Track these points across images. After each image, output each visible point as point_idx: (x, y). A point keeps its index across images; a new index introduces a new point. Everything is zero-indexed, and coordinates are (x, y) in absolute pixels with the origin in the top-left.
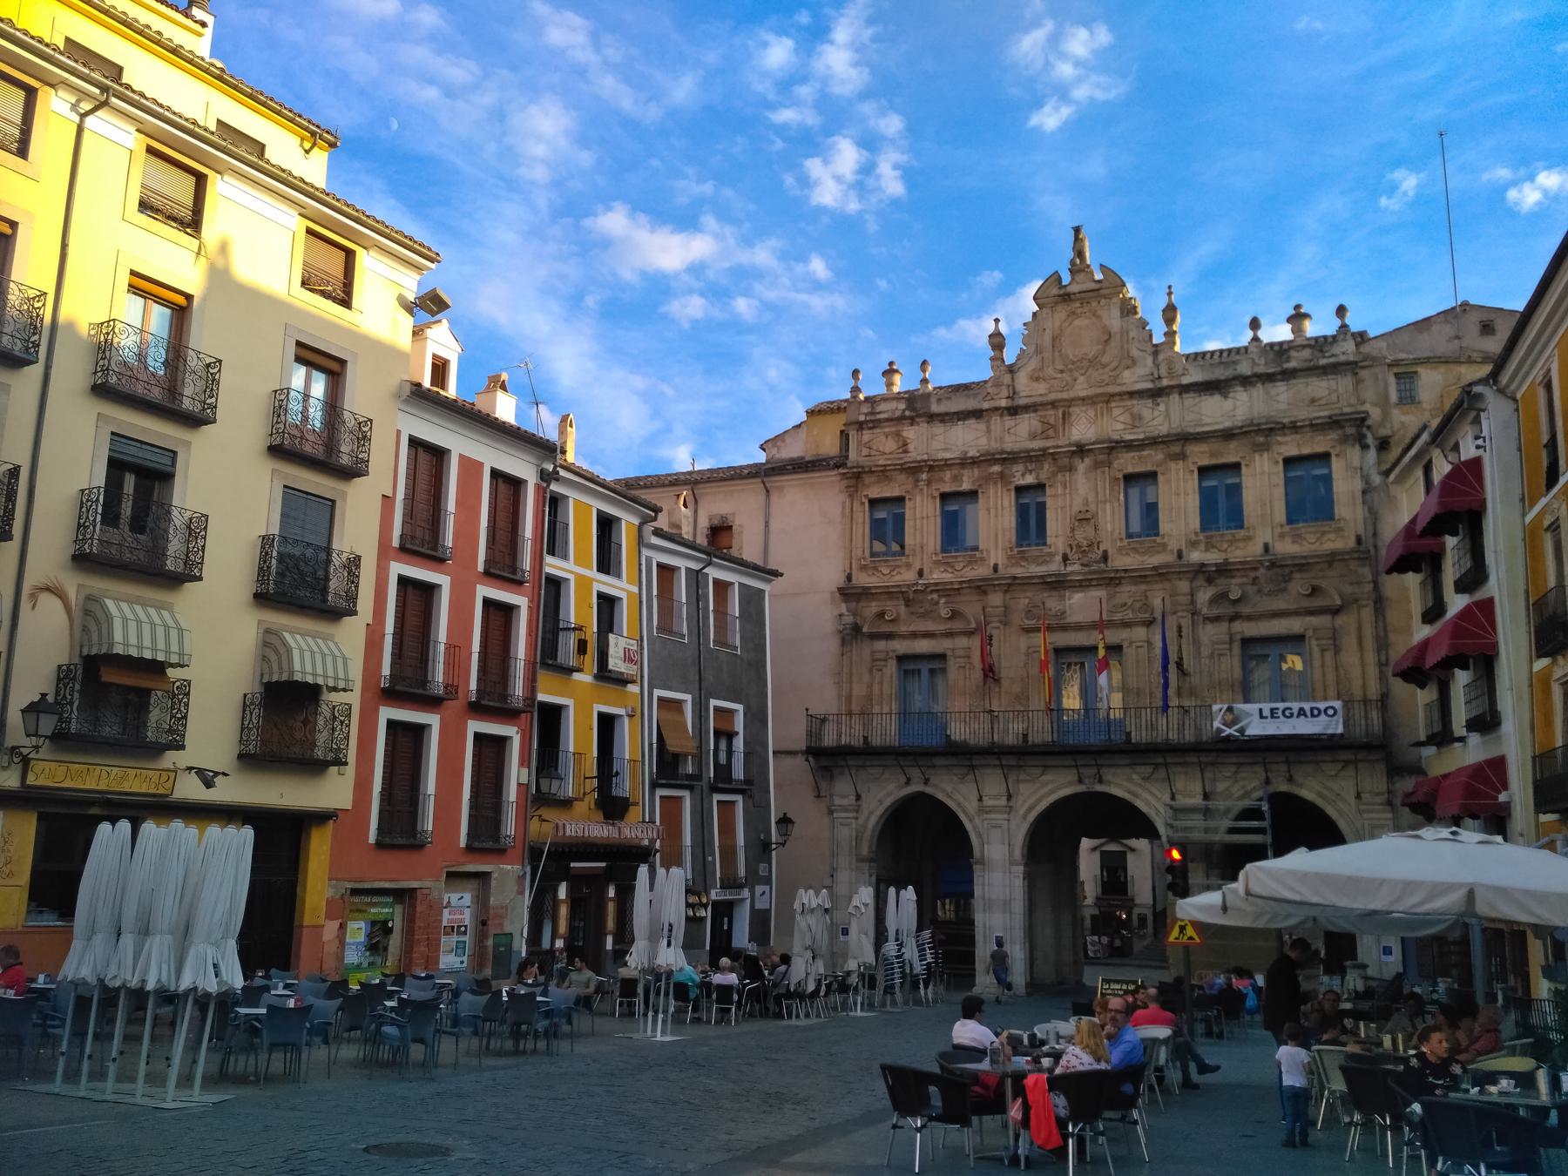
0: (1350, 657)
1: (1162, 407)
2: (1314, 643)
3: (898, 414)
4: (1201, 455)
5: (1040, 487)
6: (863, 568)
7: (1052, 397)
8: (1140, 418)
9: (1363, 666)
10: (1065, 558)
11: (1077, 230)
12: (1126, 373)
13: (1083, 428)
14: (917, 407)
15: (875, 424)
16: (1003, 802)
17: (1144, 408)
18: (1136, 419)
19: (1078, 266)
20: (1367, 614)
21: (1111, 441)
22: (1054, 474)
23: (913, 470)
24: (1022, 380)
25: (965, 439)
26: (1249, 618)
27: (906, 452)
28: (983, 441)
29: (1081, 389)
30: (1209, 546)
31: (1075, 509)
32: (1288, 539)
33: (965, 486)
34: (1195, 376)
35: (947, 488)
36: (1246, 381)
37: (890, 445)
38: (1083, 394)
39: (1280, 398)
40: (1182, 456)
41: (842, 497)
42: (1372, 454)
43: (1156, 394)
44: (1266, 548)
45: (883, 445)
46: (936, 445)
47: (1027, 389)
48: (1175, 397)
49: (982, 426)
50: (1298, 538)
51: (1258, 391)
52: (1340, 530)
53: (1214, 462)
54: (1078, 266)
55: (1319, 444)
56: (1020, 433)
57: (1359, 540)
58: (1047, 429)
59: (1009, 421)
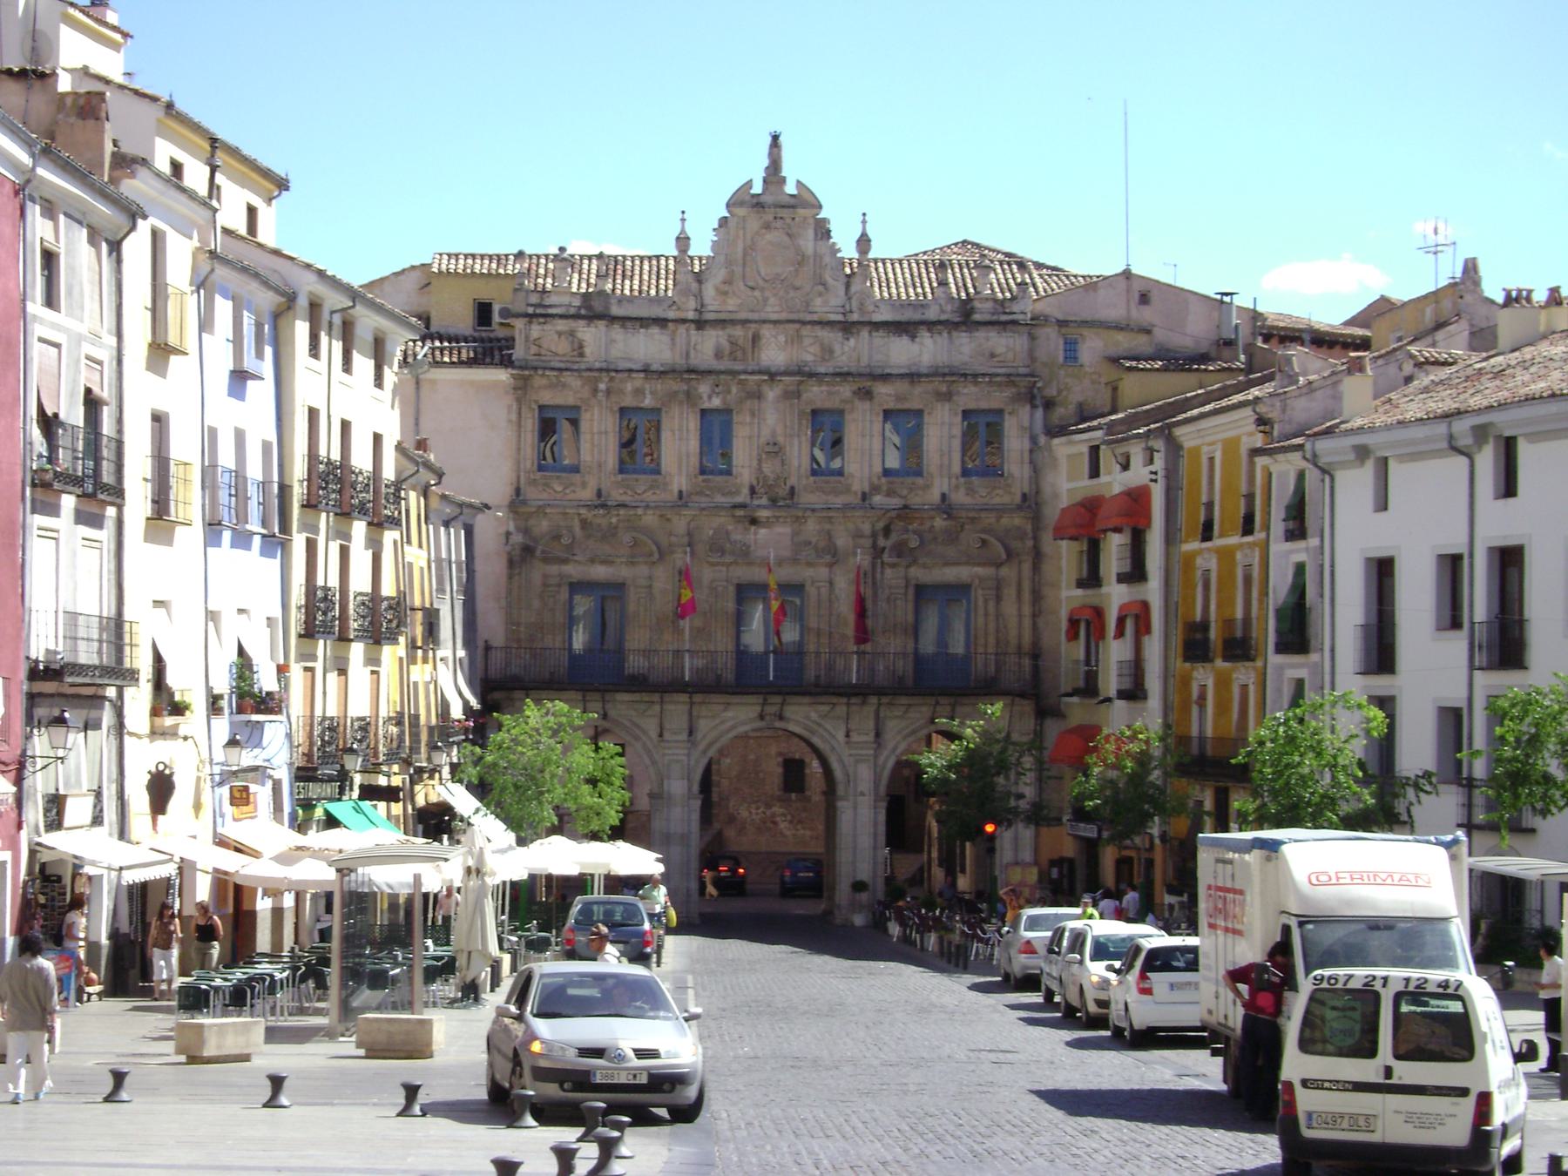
0: (1009, 608)
1: (852, 342)
2: (980, 592)
3: (572, 311)
6: (533, 482)
7: (743, 315)
8: (831, 352)
9: (1020, 616)
10: (753, 491)
11: (775, 138)
12: (818, 301)
13: (774, 353)
14: (594, 309)
16: (684, 736)
18: (827, 351)
20: (1027, 567)
21: (799, 372)
22: (741, 401)
26: (924, 566)
27: (582, 355)
29: (772, 310)
30: (889, 494)
31: (763, 440)
32: (962, 491)
33: (648, 402)
35: (628, 401)
36: (931, 325)
38: (774, 317)
41: (509, 400)
42: (1039, 413)
43: (847, 327)
44: (944, 496)
48: (865, 333)
50: (970, 491)
51: (943, 339)
52: (1009, 486)
53: (899, 406)
55: (996, 398)
56: (706, 348)
57: (1024, 496)
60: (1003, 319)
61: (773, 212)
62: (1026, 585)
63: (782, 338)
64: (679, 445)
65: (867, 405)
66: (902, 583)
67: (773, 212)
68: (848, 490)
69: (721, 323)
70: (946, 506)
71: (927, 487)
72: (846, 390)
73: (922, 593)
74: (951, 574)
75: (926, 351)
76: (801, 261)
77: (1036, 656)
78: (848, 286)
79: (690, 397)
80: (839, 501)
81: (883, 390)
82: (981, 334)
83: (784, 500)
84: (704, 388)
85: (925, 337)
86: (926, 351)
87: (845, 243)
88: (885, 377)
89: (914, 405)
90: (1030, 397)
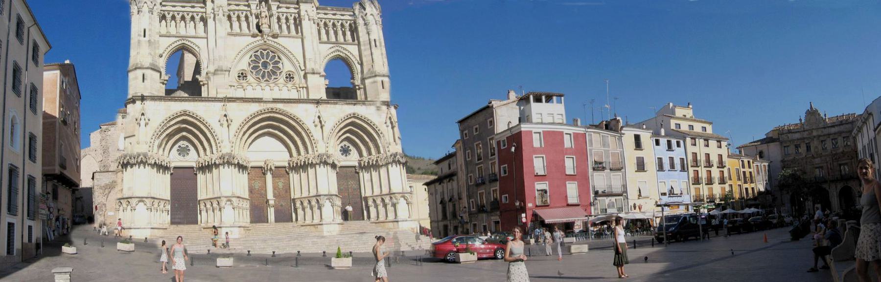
13: (815, 133)
14: (790, 132)
23: (790, 141)
47: (806, 128)
56: (805, 134)
61: (812, 113)
67: (812, 113)
73: (840, 165)
83: (820, 156)
87: (822, 115)
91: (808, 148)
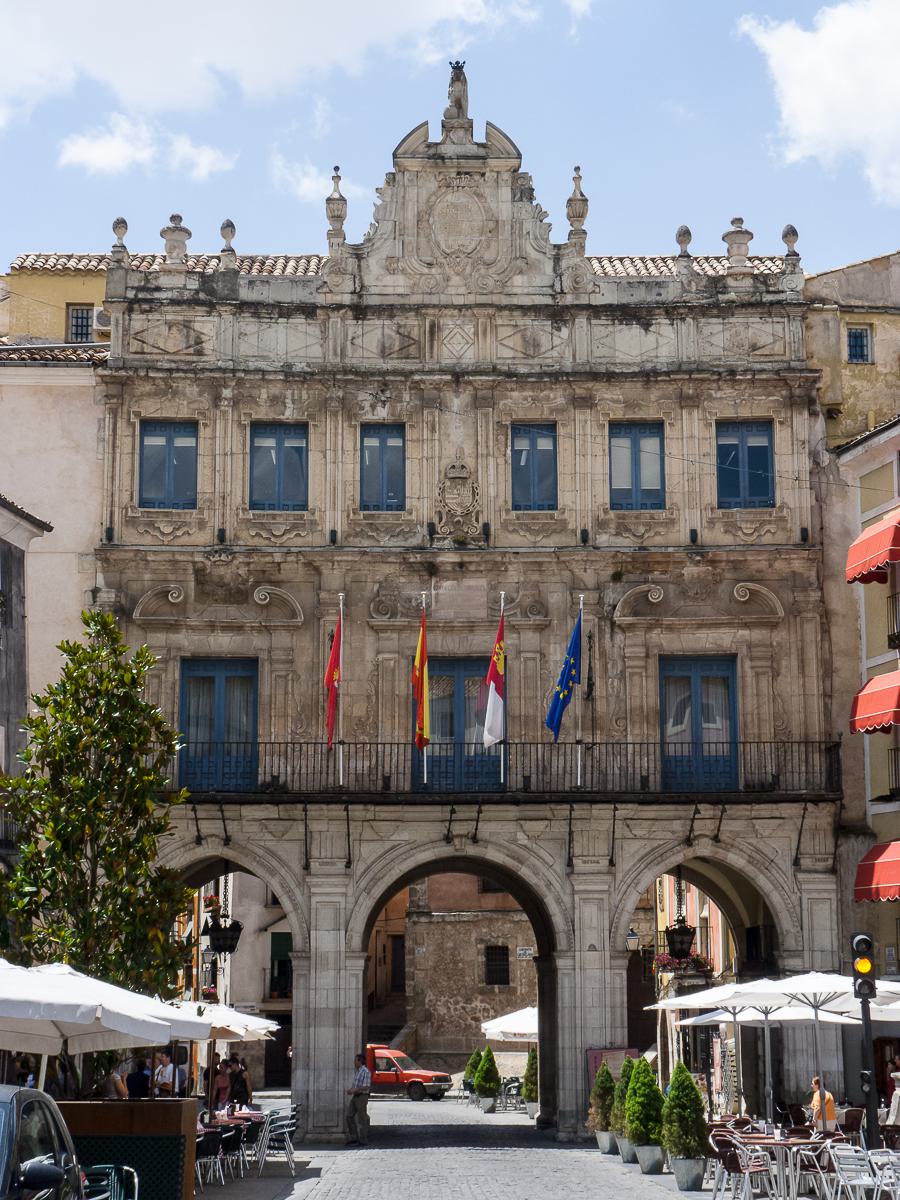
1: (565, 332)
2: (748, 664)
3: (187, 295)
4: (612, 400)
5: (398, 428)
6: (131, 522)
7: (416, 299)
8: (537, 345)
11: (458, 69)
12: (518, 280)
13: (459, 345)
14: (216, 290)
15: (152, 306)
16: (341, 865)
17: (541, 328)
18: (532, 346)
19: (457, 115)
20: (811, 631)
24: (374, 265)
25: (292, 343)
26: (670, 628)
27: (200, 353)
28: (316, 351)
29: (457, 291)
30: (622, 529)
31: (445, 462)
32: (719, 527)
33: (289, 414)
34: (608, 296)
35: (263, 413)
36: (672, 311)
37: (174, 342)
38: (460, 301)
39: (714, 340)
40: (586, 402)
41: (99, 411)
42: (821, 421)
43: (558, 315)
44: (694, 533)
45: (161, 335)
46: (246, 348)
47: (383, 284)
48: (581, 321)
49: (314, 330)
50: (731, 527)
51: (688, 326)
52: (783, 519)
53: (630, 416)
54: (457, 115)
55: (759, 405)
56: (368, 343)
57: (804, 531)
58: (408, 345)
59: (353, 327)
60: (765, 297)
62: (812, 653)
63: (470, 329)
64: (334, 469)
65: (588, 414)
66: (641, 651)
67: (458, 156)
68: (562, 527)
69: (387, 310)
70: (695, 546)
71: (672, 522)
72: (558, 396)
74: (706, 640)
75: (664, 343)
76: (494, 226)
77: (832, 749)
78: (557, 259)
79: (348, 409)
80: (552, 542)
81: (606, 394)
82: (737, 320)
83: (473, 543)
84: (364, 397)
85: (663, 326)
86: (664, 343)
88: (610, 377)
89: (650, 413)
90: (808, 403)
91: (382, 490)
